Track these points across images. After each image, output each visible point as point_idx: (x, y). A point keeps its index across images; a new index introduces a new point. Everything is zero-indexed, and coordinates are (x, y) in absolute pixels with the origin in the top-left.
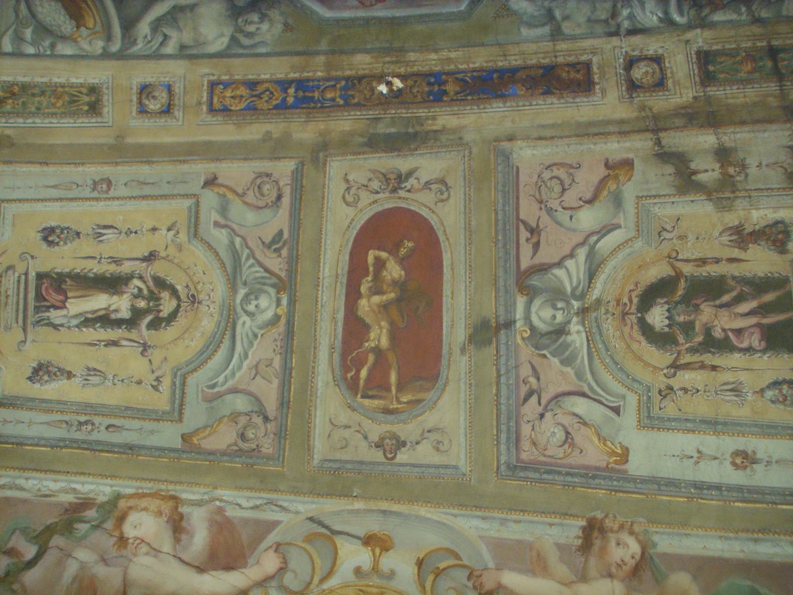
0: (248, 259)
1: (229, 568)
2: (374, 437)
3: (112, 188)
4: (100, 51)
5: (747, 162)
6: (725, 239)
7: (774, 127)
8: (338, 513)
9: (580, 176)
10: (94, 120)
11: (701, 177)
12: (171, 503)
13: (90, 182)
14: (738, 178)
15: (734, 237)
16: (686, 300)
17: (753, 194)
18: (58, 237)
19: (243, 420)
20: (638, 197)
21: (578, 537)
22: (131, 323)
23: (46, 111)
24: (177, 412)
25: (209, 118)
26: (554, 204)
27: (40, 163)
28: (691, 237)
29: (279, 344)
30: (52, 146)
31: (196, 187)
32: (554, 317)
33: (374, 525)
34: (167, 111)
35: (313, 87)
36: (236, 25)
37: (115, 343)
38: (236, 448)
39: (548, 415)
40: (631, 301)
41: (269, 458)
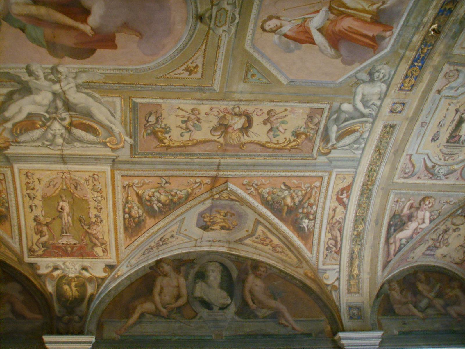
4: (371, 125)
30: (402, 139)
31: (438, 96)
34: (403, 104)
35: (418, 56)
36: (377, 81)
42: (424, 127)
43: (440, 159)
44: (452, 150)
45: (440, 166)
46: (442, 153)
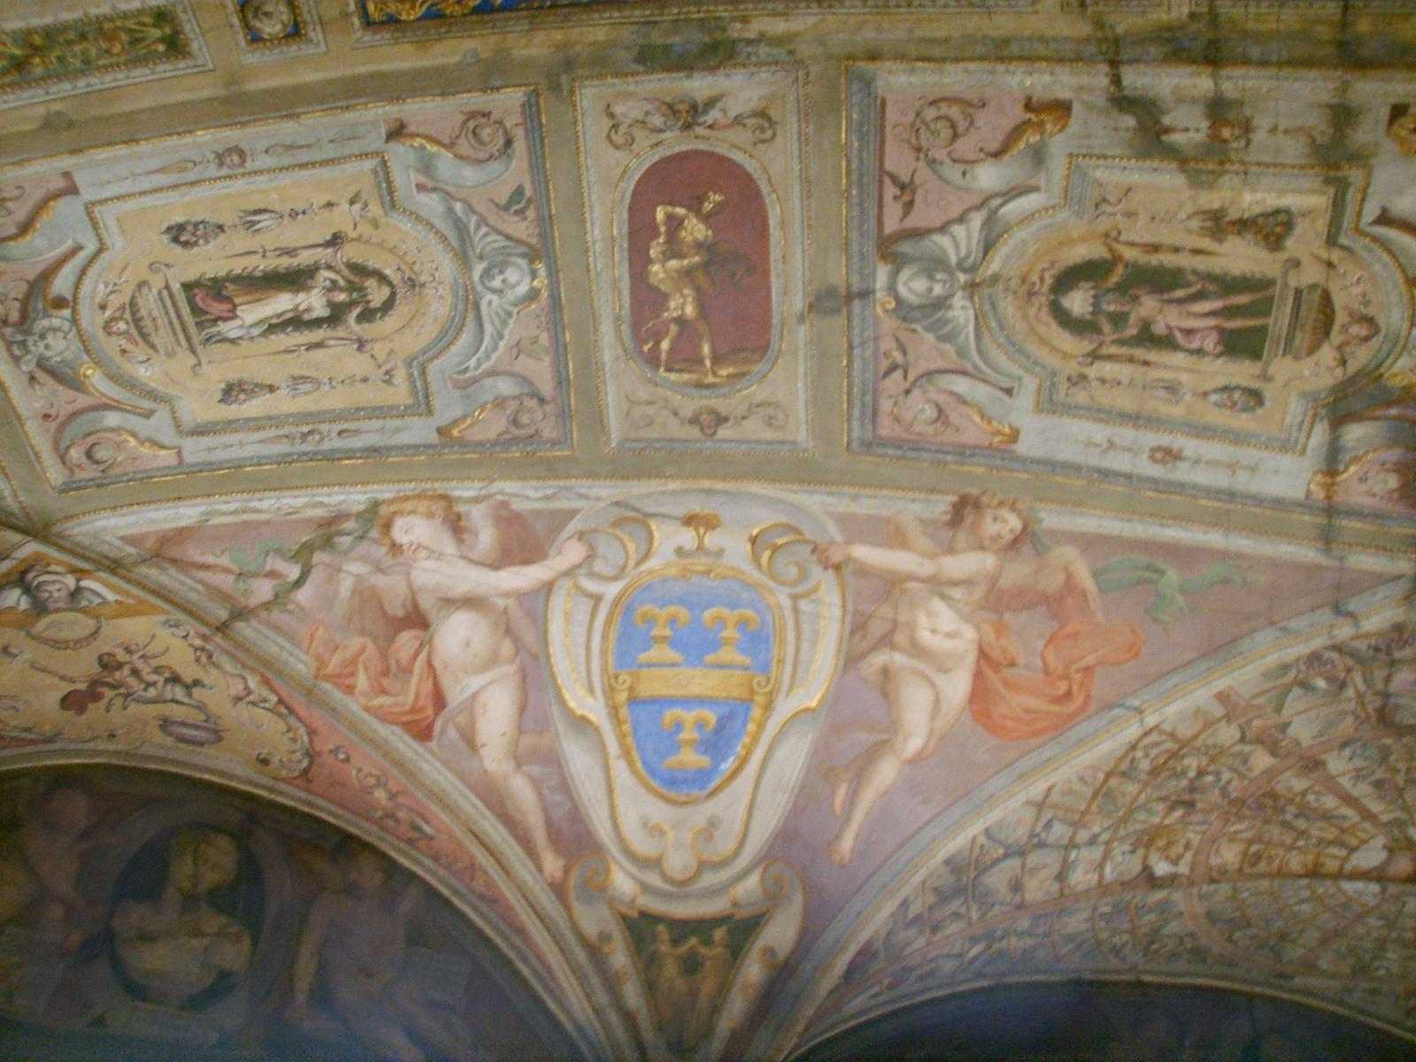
0: (478, 226)
1: (527, 562)
2: (687, 412)
3: (249, 159)
5: (1255, 122)
6: (1195, 224)
7: (1314, 73)
8: (650, 495)
9: (982, 118)
10: (182, 65)
11: (1176, 138)
12: (442, 503)
13: (211, 157)
14: (1235, 145)
15: (1208, 224)
16: (1122, 288)
17: (1253, 169)
18: (194, 234)
19: (512, 406)
20: (1071, 155)
21: (946, 513)
22: (336, 316)
23: (101, 63)
24: (423, 404)
25: (368, 37)
26: (939, 154)
27: (124, 142)
28: (1143, 216)
29: (543, 319)
31: (376, 140)
32: (930, 290)
33: (696, 506)
34: (295, 32)
37: (319, 345)
38: (508, 436)
39: (916, 392)
40: (1042, 279)
41: (554, 443)
42: (221, 164)
43: (103, 307)
44: (162, 322)
45: (74, 321)
46: (133, 298)
